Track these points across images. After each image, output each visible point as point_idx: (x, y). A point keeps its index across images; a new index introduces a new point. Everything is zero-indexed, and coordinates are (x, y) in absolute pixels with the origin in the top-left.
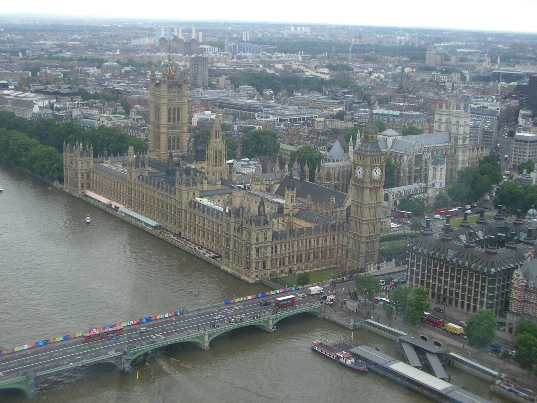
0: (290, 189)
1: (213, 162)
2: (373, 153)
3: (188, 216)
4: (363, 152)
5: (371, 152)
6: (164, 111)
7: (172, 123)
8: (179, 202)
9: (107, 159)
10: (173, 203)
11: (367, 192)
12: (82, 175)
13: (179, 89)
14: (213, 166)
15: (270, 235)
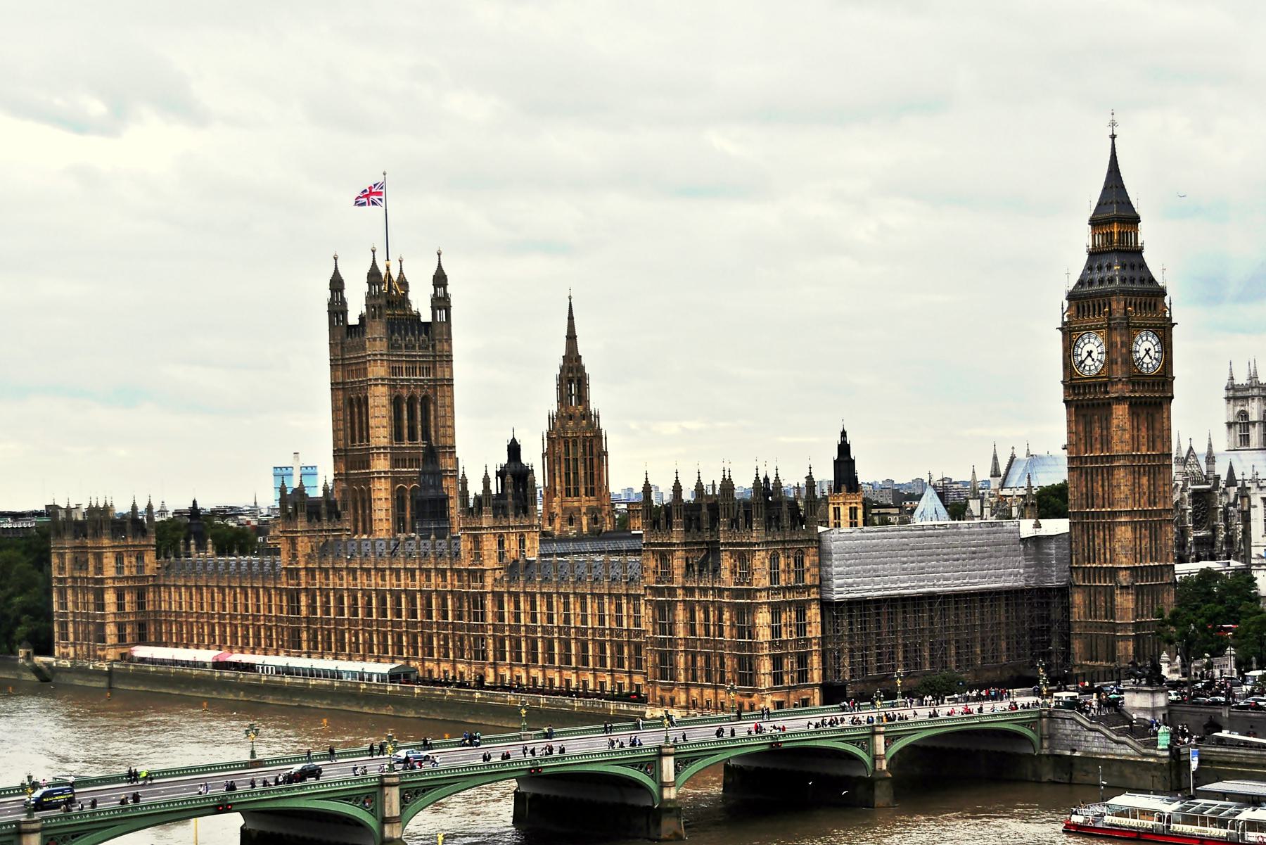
0: (844, 488)
1: (568, 482)
2: (1128, 285)
3: (508, 607)
4: (1096, 288)
5: (1123, 280)
6: (379, 400)
7: (406, 443)
8: (475, 571)
9: (201, 546)
10: (452, 583)
11: (1120, 413)
12: (120, 597)
13: (424, 335)
14: (568, 495)
15: (812, 564)
